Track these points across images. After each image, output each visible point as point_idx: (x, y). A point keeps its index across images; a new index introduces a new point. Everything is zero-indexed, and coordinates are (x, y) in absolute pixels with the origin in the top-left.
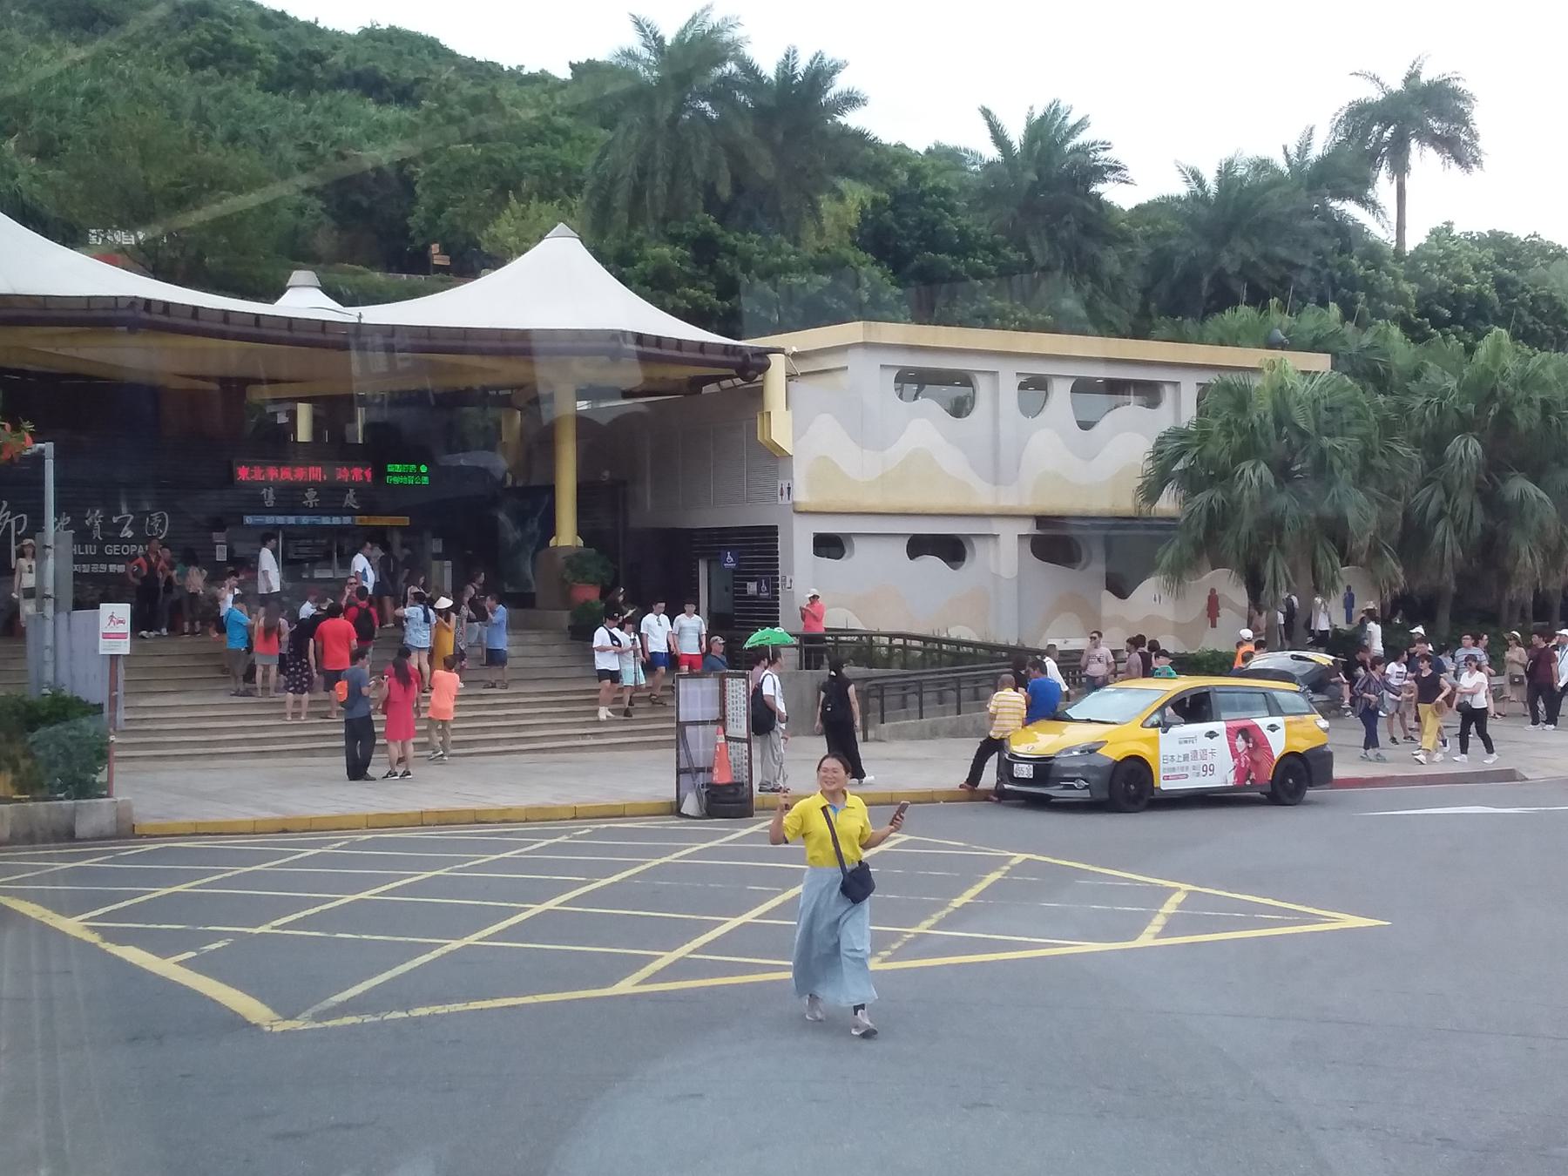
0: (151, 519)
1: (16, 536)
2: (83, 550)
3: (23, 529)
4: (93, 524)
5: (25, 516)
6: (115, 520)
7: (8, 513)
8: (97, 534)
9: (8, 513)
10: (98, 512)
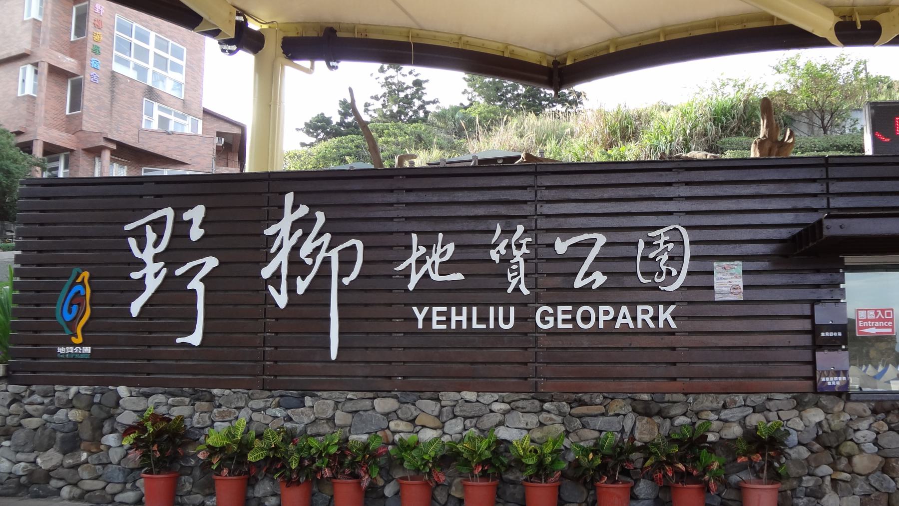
1: (341, 289)
2: (483, 319)
3: (354, 275)
4: (506, 260)
5: (360, 245)
6: (561, 247)
7: (327, 238)
9: (327, 238)
10: (520, 229)
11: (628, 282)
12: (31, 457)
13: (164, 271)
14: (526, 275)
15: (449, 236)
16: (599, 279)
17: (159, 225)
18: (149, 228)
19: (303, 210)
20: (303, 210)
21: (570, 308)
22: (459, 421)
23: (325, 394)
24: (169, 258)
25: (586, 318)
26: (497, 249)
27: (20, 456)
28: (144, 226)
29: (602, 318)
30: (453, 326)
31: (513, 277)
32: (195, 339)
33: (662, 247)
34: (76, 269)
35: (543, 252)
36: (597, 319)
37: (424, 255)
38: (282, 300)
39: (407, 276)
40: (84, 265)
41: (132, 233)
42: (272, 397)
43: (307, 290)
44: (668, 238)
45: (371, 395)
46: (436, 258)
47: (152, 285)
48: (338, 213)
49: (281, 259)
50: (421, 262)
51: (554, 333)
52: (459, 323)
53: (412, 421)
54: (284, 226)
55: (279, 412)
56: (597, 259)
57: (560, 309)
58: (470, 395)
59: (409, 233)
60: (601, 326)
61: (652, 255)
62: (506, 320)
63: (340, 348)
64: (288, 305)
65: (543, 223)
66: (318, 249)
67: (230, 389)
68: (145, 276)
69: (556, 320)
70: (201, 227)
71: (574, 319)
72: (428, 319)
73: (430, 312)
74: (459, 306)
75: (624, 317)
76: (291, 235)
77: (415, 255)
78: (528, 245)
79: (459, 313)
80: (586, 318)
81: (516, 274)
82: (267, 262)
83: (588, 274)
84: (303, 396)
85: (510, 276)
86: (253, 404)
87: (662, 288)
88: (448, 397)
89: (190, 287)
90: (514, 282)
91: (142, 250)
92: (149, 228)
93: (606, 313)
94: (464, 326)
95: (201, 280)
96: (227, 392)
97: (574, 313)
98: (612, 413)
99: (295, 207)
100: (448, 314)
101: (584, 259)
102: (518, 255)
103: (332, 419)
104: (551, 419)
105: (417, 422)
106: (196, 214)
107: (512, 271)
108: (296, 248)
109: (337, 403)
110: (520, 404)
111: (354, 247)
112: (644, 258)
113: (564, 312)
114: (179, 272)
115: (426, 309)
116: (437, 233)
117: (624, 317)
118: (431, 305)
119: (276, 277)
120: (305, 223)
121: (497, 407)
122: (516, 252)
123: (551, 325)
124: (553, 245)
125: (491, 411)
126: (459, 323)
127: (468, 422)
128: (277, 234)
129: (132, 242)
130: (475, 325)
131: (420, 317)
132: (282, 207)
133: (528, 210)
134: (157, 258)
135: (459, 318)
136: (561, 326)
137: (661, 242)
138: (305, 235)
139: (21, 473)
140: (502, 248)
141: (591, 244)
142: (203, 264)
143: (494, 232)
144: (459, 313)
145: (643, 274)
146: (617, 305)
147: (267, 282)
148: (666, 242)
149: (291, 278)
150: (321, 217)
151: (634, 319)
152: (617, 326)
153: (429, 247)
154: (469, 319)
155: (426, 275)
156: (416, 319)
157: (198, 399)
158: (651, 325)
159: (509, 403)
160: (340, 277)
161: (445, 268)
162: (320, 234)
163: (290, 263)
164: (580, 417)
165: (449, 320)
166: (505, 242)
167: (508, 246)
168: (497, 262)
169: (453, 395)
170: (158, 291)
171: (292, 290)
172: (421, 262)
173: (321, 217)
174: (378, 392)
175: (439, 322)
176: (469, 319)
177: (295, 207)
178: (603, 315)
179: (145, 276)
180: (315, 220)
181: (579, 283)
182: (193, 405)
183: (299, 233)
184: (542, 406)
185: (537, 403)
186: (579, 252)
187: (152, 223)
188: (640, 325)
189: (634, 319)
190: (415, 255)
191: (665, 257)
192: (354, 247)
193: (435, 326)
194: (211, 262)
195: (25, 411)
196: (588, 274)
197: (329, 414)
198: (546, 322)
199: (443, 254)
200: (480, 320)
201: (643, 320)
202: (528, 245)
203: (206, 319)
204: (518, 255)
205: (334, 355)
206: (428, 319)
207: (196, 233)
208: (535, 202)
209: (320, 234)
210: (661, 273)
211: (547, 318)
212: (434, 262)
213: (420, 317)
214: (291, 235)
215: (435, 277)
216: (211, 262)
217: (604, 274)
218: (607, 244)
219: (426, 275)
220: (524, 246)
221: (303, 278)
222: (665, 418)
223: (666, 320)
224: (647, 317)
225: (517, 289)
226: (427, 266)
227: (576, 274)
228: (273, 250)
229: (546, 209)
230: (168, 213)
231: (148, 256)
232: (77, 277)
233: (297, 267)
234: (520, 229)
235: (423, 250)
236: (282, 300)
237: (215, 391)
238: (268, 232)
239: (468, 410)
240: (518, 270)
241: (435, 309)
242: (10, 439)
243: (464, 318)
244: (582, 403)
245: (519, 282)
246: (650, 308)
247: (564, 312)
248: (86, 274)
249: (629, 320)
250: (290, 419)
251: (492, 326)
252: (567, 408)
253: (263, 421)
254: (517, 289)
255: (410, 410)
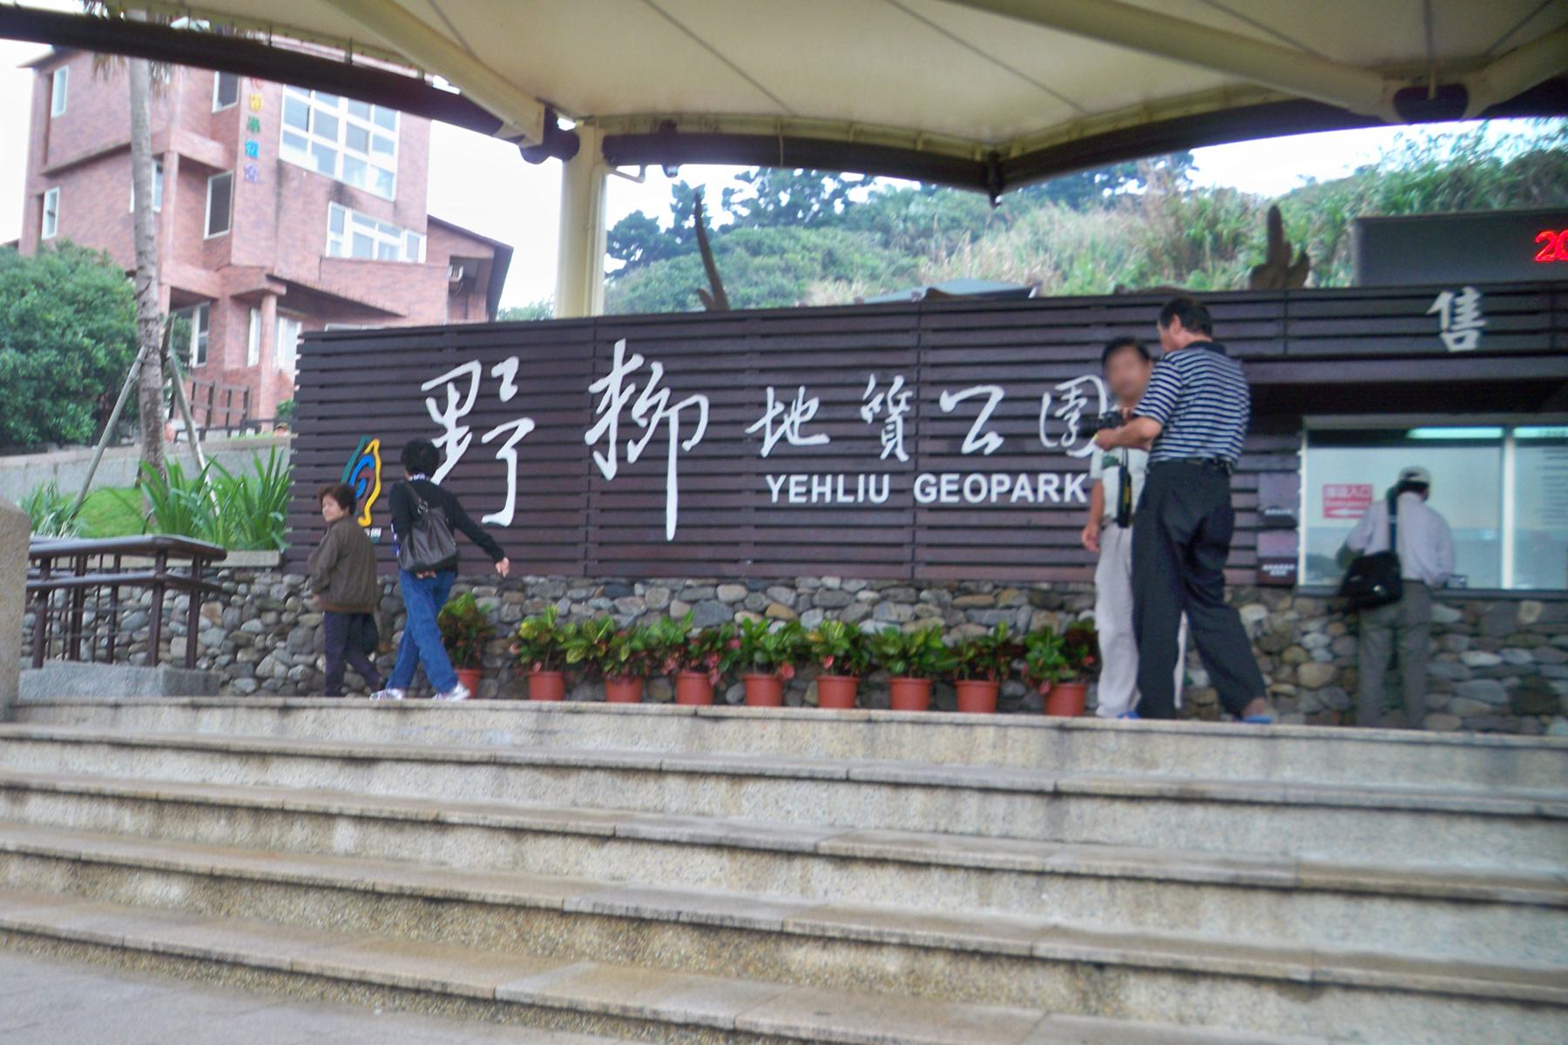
0: (1057, 400)
1: (682, 457)
4: (880, 420)
5: (704, 402)
6: (948, 402)
7: (664, 394)
8: (893, 444)
9: (664, 394)
10: (899, 381)
11: (1030, 446)
12: (311, 659)
13: (469, 437)
14: (905, 438)
15: (811, 391)
16: (994, 442)
17: (463, 382)
18: (451, 387)
19: (637, 361)
20: (637, 361)
21: (956, 477)
22: (819, 612)
23: (659, 581)
24: (477, 421)
25: (976, 490)
26: (870, 405)
27: (297, 658)
28: (447, 382)
29: (995, 490)
30: (814, 498)
31: (888, 440)
32: (505, 517)
33: (1072, 403)
34: (363, 439)
35: (926, 410)
36: (989, 491)
37: (782, 414)
38: (609, 469)
39: (760, 439)
40: (374, 433)
41: (431, 393)
42: (597, 585)
43: (640, 458)
44: (1079, 392)
45: (714, 581)
46: (795, 417)
47: (454, 454)
48: (678, 365)
49: (610, 420)
50: (777, 422)
51: (936, 508)
52: (822, 495)
53: (762, 613)
54: (614, 380)
55: (604, 603)
56: (992, 418)
57: (945, 478)
58: (832, 582)
59: (764, 388)
60: (994, 498)
61: (1059, 413)
62: (879, 492)
63: (678, 527)
64: (617, 476)
65: (928, 374)
66: (653, 408)
67: (545, 576)
68: (445, 445)
69: (939, 491)
70: (513, 383)
71: (960, 492)
72: (784, 491)
73: (787, 482)
74: (822, 475)
75: (1023, 488)
76: (622, 391)
77: (771, 413)
78: (908, 401)
79: (822, 483)
80: (976, 490)
81: (891, 435)
82: (592, 424)
83: (979, 436)
84: (633, 584)
85: (884, 438)
86: (575, 594)
87: (1070, 453)
88: (806, 583)
89: (500, 455)
90: (891, 444)
91: (443, 412)
92: (451, 387)
93: (1001, 483)
94: (828, 498)
95: (515, 446)
96: (542, 580)
97: (961, 482)
98: (1001, 604)
99: (627, 358)
100: (808, 484)
101: (974, 419)
102: (895, 414)
103: (666, 610)
104: (928, 611)
105: (768, 613)
106: (508, 368)
107: (887, 432)
108: (627, 408)
109: (673, 592)
110: (892, 591)
111: (696, 406)
112: (1050, 417)
113: (949, 482)
114: (487, 438)
115: (782, 479)
116: (798, 387)
117: (1023, 488)
118: (789, 474)
119: (603, 442)
120: (641, 376)
121: (863, 595)
122: (892, 409)
123: (932, 497)
124: (937, 401)
125: (858, 601)
126: (822, 495)
127: (828, 614)
128: (605, 391)
129: (431, 404)
130: (842, 498)
131: (775, 488)
132: (610, 358)
133: (909, 358)
134: (460, 422)
135: (822, 489)
136: (945, 499)
137: (1072, 396)
138: (639, 391)
139: (298, 677)
140: (875, 404)
141: (984, 399)
142: (516, 428)
143: (866, 385)
144: (822, 483)
145: (1050, 436)
146: (1014, 474)
147: (592, 448)
148: (1077, 397)
149: (622, 443)
150: (657, 369)
151: (1035, 491)
152: (1014, 498)
153: (788, 405)
154: (834, 491)
155: (783, 439)
156: (769, 492)
157: (508, 589)
158: (1055, 498)
159: (879, 591)
160: (680, 441)
161: (807, 428)
162: (656, 390)
163: (621, 425)
164: (965, 609)
165: (809, 492)
166: (879, 397)
167: (884, 403)
168: (870, 420)
169: (812, 582)
170: (460, 462)
171: (622, 458)
172: (777, 422)
173: (657, 369)
174: (724, 579)
175: (797, 494)
176: (834, 491)
177: (627, 358)
178: (997, 486)
179: (445, 445)
180: (650, 373)
181: (968, 446)
182: (501, 596)
183: (631, 389)
184: (918, 596)
185: (912, 591)
186: (969, 410)
187: (455, 381)
188: (1041, 498)
189: (1035, 491)
190: (771, 413)
191: (1075, 416)
192: (696, 406)
193: (793, 499)
194: (525, 426)
195: (304, 606)
196: (979, 436)
197: (664, 603)
198: (928, 494)
199: (804, 412)
200: (847, 492)
201: (1046, 494)
202: (908, 401)
203: (518, 494)
204: (895, 414)
205: (671, 533)
206: (784, 491)
207: (507, 392)
208: (918, 348)
209: (656, 390)
210: (1069, 436)
211: (928, 490)
212: (793, 423)
213: (775, 488)
214: (622, 391)
215: (795, 440)
216: (525, 426)
217: (1000, 435)
218: (1004, 400)
219: (783, 439)
220: (903, 403)
221: (636, 442)
222: (1069, 612)
223: (1073, 494)
224: (1051, 489)
225: (892, 456)
226: (785, 427)
227: (964, 437)
228: (600, 410)
229: (932, 357)
230: (475, 368)
231: (449, 418)
232: (365, 447)
233: (628, 429)
234: (899, 381)
235: (780, 407)
236: (609, 469)
237: (529, 579)
238: (595, 388)
239: (831, 599)
240: (894, 430)
241: (793, 479)
242: (285, 640)
243: (827, 489)
244: (968, 592)
245: (896, 446)
246: (1055, 478)
247: (949, 482)
248: (376, 444)
249: (1028, 493)
250: (616, 611)
251: (861, 497)
252: (947, 597)
253: (584, 613)
254: (892, 456)
255: (762, 600)
